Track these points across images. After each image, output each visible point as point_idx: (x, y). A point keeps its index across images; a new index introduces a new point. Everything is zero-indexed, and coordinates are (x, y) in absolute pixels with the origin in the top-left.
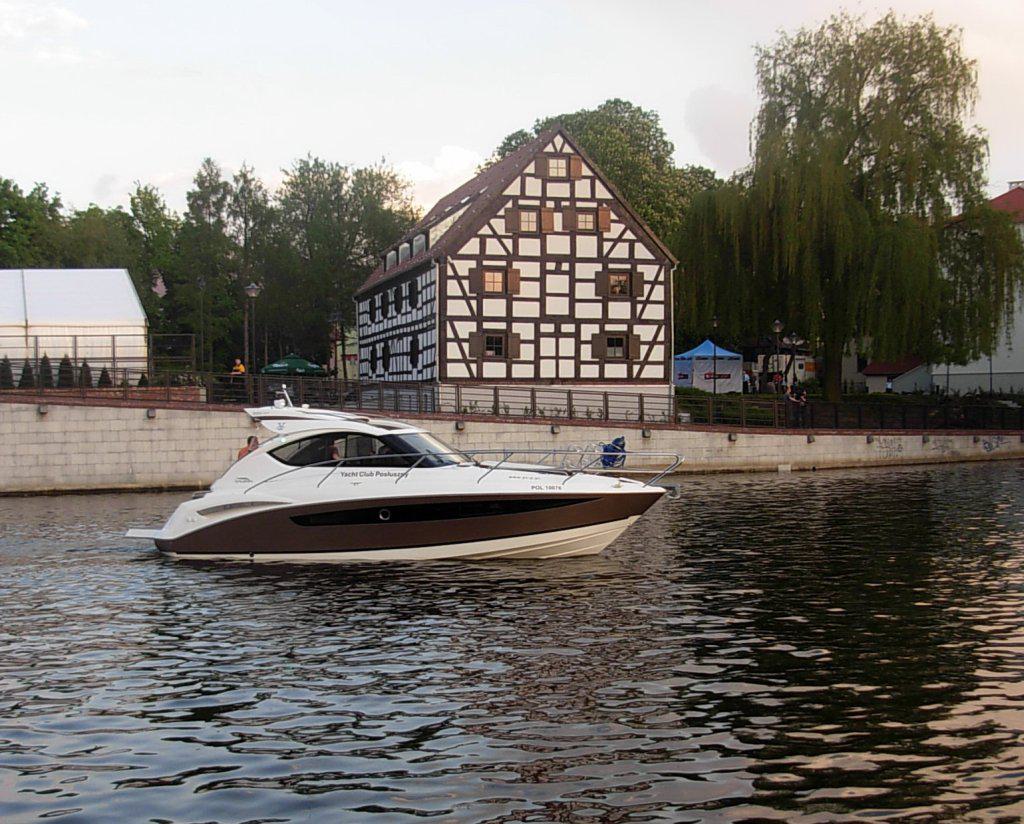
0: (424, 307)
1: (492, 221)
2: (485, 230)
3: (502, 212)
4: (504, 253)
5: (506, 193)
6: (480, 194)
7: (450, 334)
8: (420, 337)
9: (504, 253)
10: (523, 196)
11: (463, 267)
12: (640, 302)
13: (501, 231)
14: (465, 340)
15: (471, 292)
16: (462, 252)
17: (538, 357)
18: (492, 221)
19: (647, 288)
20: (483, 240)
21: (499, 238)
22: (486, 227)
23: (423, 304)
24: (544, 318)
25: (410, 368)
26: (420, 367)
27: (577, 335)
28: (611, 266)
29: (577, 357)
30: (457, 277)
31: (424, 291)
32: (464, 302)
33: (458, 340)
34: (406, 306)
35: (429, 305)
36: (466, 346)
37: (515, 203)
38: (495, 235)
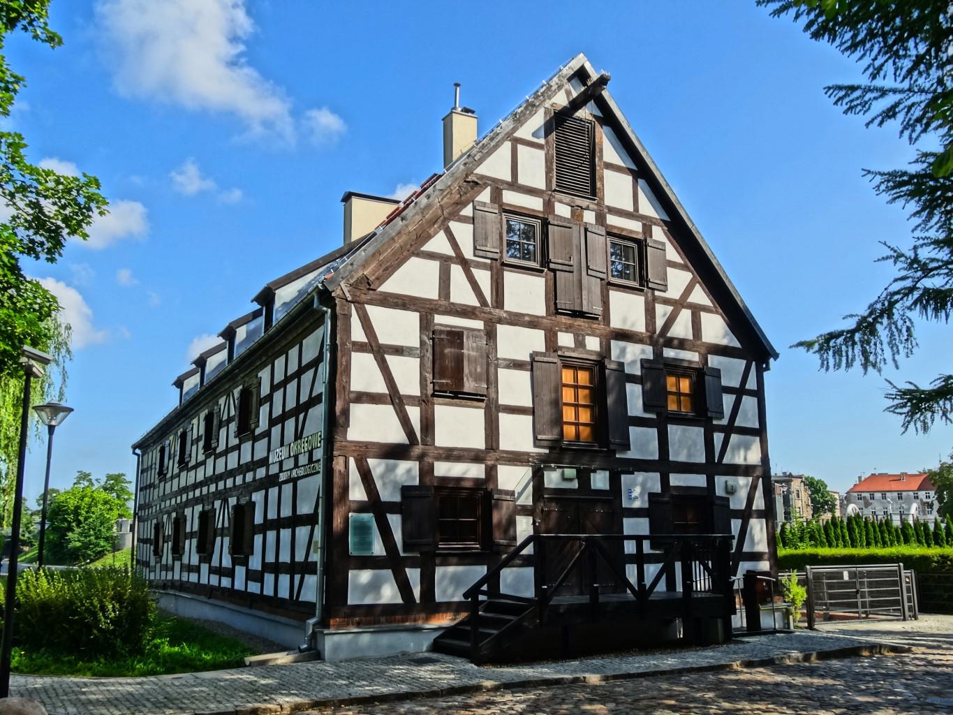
0: (276, 431)
1: (453, 225)
2: (439, 244)
3: (468, 211)
4: (473, 301)
5: (482, 170)
8: (257, 497)
9: (473, 301)
10: (514, 185)
12: (720, 429)
14: (392, 507)
16: (389, 286)
18: (453, 225)
19: (728, 401)
21: (465, 264)
22: (441, 235)
23: (272, 422)
26: (255, 563)
28: (669, 353)
30: (380, 352)
31: (278, 396)
32: (388, 410)
34: (227, 436)
35: (290, 424)
36: (395, 521)
37: (496, 197)
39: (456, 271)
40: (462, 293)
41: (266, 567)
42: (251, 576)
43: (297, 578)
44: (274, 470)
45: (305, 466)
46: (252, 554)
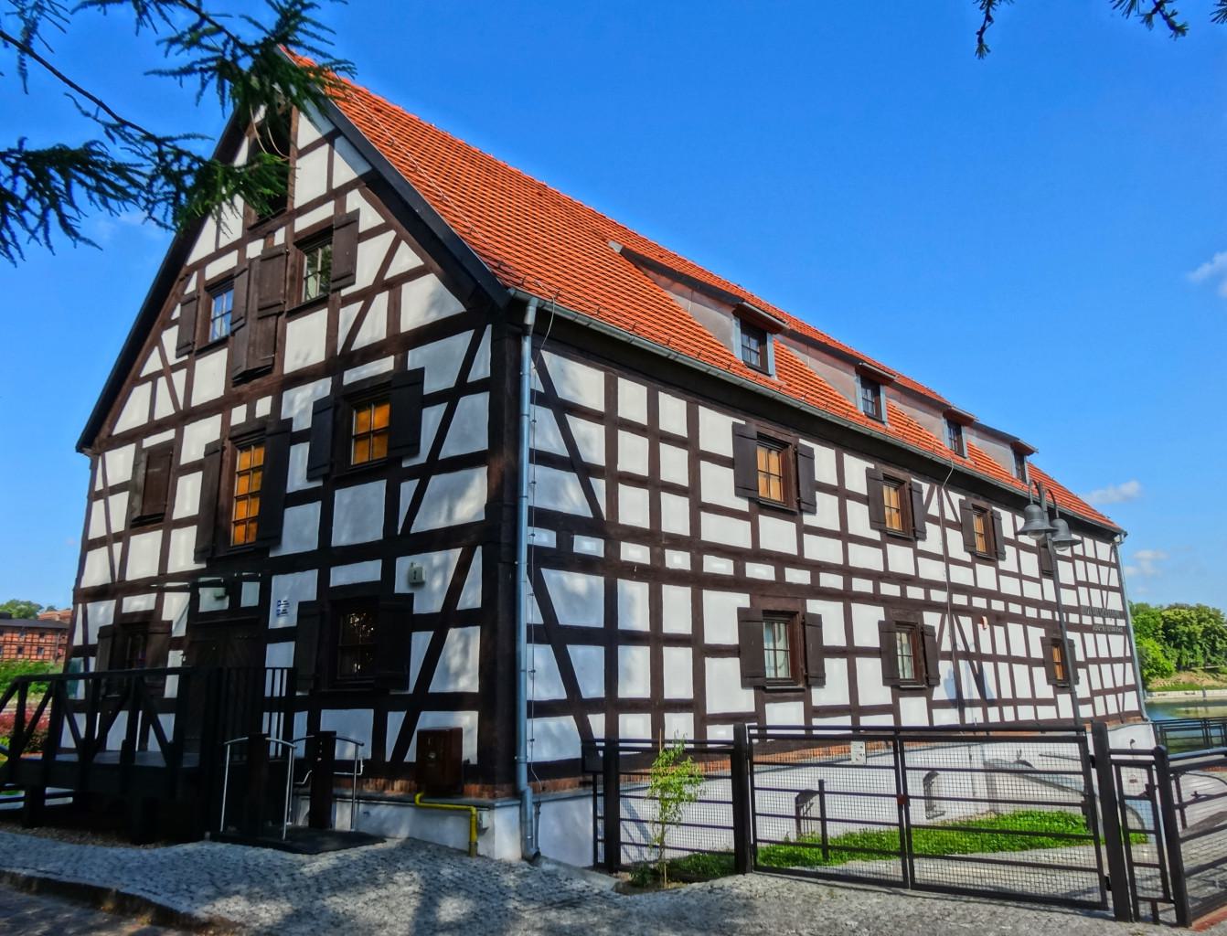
25: (1045, 691)
26: (1082, 690)
41: (1094, 693)
46: (1078, 683)
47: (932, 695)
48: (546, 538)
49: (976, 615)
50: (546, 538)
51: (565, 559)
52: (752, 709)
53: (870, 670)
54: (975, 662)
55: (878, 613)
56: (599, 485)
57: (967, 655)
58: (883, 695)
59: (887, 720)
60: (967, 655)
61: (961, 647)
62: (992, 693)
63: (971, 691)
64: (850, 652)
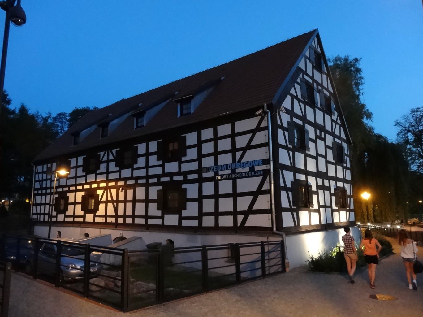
1: (296, 85)
6: (221, 80)
7: (282, 184)
11: (285, 119)
13: (300, 97)
15: (289, 144)
17: (320, 207)
18: (296, 85)
20: (293, 97)
21: (299, 101)
22: (293, 88)
24: (318, 174)
27: (329, 188)
29: (331, 207)
30: (284, 129)
33: (286, 189)
38: (297, 98)
39: (296, 102)
40: (297, 110)
41: (201, 214)
42: (181, 219)
43: (240, 218)
44: (205, 175)
45: (246, 172)
47: (96, 213)
48: (36, 192)
49: (117, 188)
50: (36, 192)
51: (38, 194)
52: (55, 215)
53: (79, 207)
54: (115, 204)
55: (83, 193)
56: (41, 183)
57: (112, 201)
58: (82, 213)
59: (81, 220)
60: (112, 201)
61: (109, 199)
62: (121, 212)
63: (111, 211)
64: (75, 203)
